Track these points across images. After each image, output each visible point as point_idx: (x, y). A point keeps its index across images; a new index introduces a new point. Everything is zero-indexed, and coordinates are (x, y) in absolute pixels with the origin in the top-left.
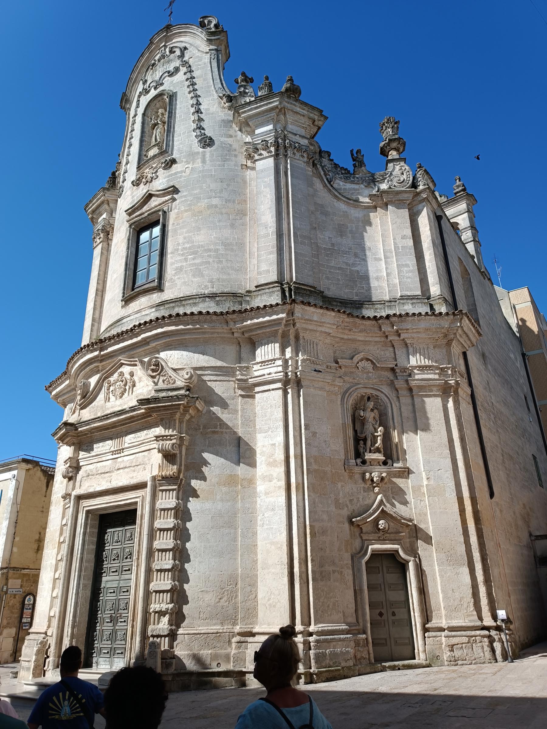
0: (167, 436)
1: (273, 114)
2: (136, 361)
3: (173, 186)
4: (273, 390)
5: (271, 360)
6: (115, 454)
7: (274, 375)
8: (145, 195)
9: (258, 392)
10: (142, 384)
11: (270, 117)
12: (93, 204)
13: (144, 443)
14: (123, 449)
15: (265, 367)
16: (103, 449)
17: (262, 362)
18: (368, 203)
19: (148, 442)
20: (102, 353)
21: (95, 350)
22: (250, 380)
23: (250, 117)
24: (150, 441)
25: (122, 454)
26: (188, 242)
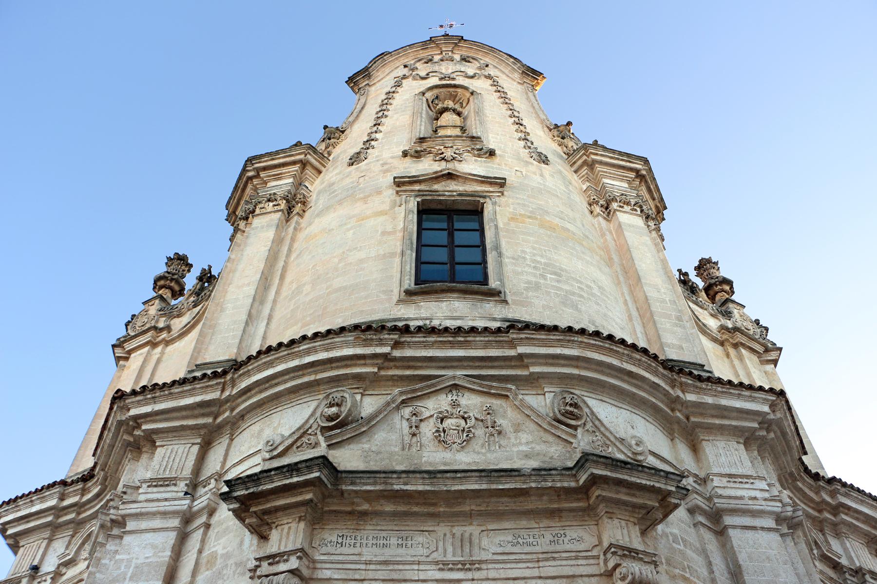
0: (637, 552)
1: (632, 175)
2: (510, 390)
3: (505, 179)
4: (762, 528)
5: (747, 477)
6: (451, 570)
7: (763, 503)
8: (441, 171)
9: (734, 527)
10: (524, 437)
11: (626, 177)
12: (260, 162)
13: (554, 559)
14: (472, 563)
15: (737, 485)
16: (401, 551)
17: (730, 476)
18: (717, 335)
19: (567, 559)
20: (397, 353)
21: (381, 343)
22: (716, 500)
23: (601, 163)
24: (577, 558)
25: (477, 575)
26: (542, 256)
